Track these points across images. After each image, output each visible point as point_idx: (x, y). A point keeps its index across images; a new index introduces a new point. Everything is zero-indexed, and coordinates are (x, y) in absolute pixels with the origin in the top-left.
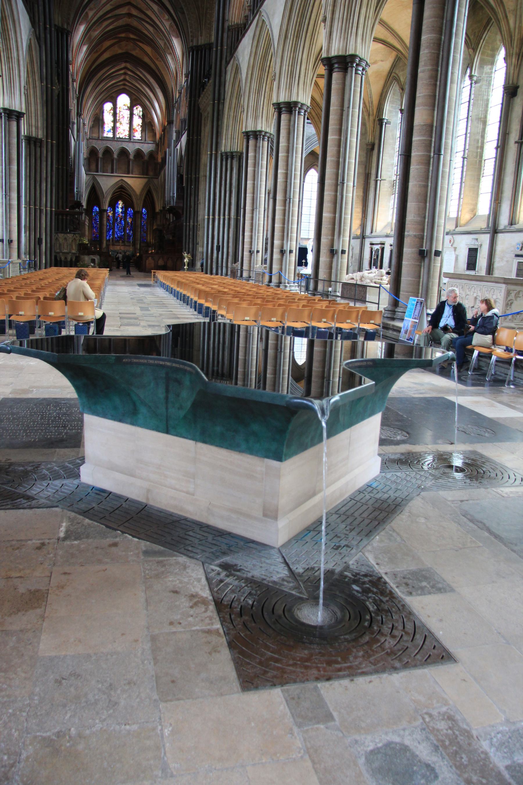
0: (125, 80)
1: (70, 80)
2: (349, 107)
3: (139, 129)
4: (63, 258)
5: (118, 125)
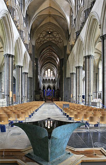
3: (52, 75)
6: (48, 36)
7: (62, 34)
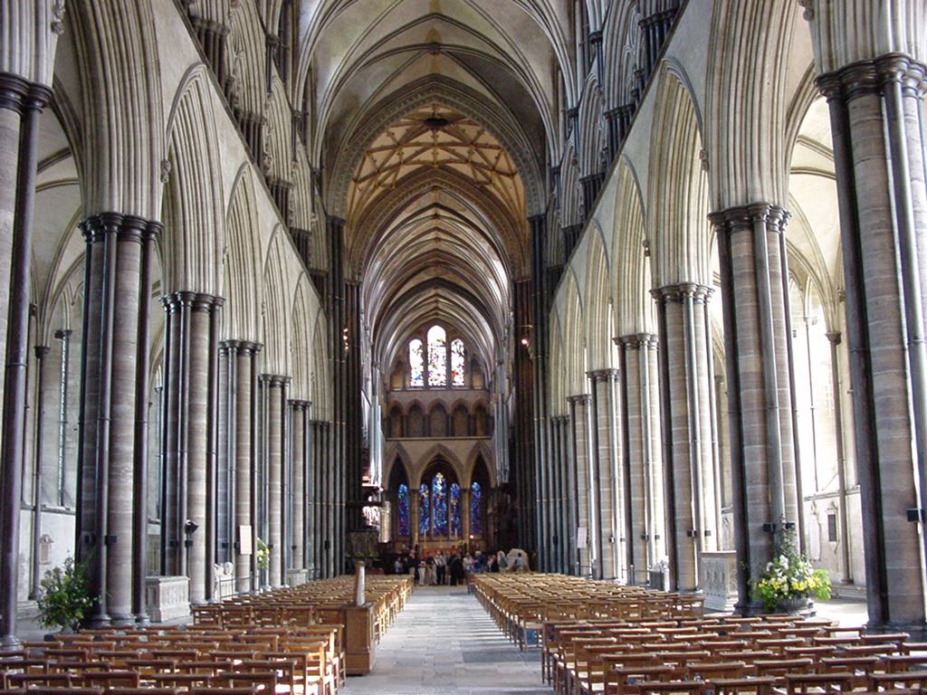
0: (437, 308)
2: (645, 385)
3: (461, 371)
5: (430, 368)
6: (426, 137)
7: (515, 144)
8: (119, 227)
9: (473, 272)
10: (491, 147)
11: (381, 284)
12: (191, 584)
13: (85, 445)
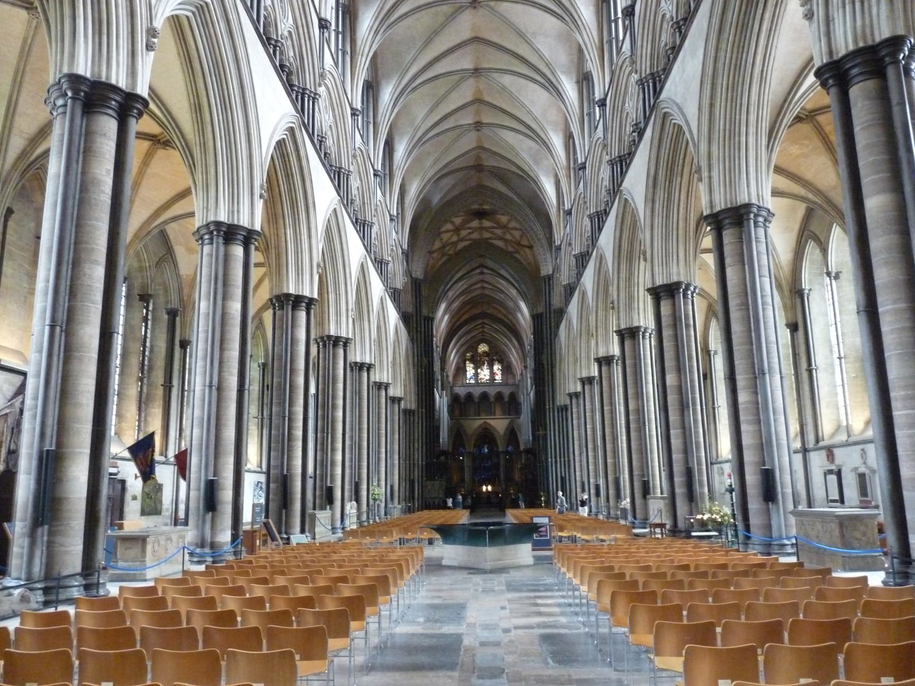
0: (483, 332)
1: (434, 346)
3: (499, 373)
4: (431, 503)
6: (475, 224)
8: (293, 301)
9: (506, 308)
10: (517, 229)
11: (446, 317)
12: (333, 515)
13: (273, 432)
